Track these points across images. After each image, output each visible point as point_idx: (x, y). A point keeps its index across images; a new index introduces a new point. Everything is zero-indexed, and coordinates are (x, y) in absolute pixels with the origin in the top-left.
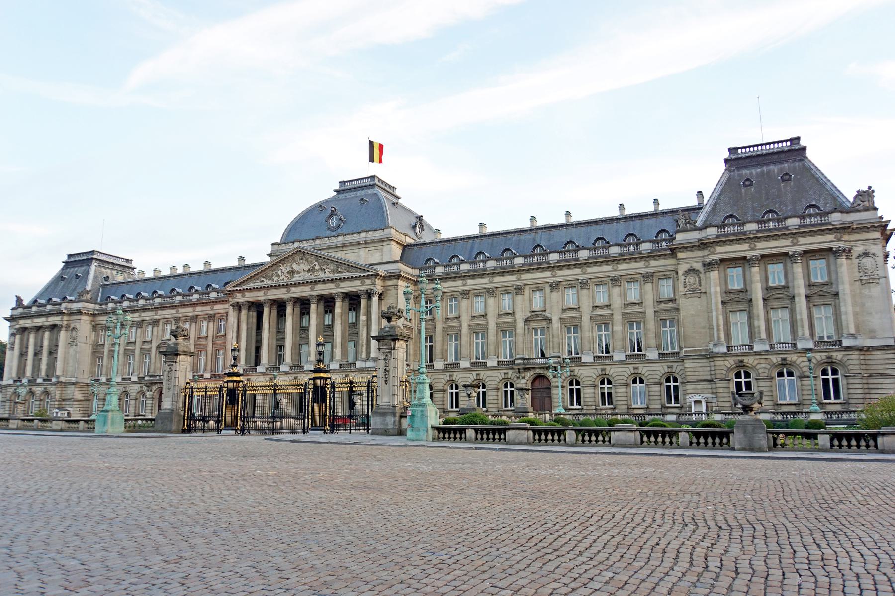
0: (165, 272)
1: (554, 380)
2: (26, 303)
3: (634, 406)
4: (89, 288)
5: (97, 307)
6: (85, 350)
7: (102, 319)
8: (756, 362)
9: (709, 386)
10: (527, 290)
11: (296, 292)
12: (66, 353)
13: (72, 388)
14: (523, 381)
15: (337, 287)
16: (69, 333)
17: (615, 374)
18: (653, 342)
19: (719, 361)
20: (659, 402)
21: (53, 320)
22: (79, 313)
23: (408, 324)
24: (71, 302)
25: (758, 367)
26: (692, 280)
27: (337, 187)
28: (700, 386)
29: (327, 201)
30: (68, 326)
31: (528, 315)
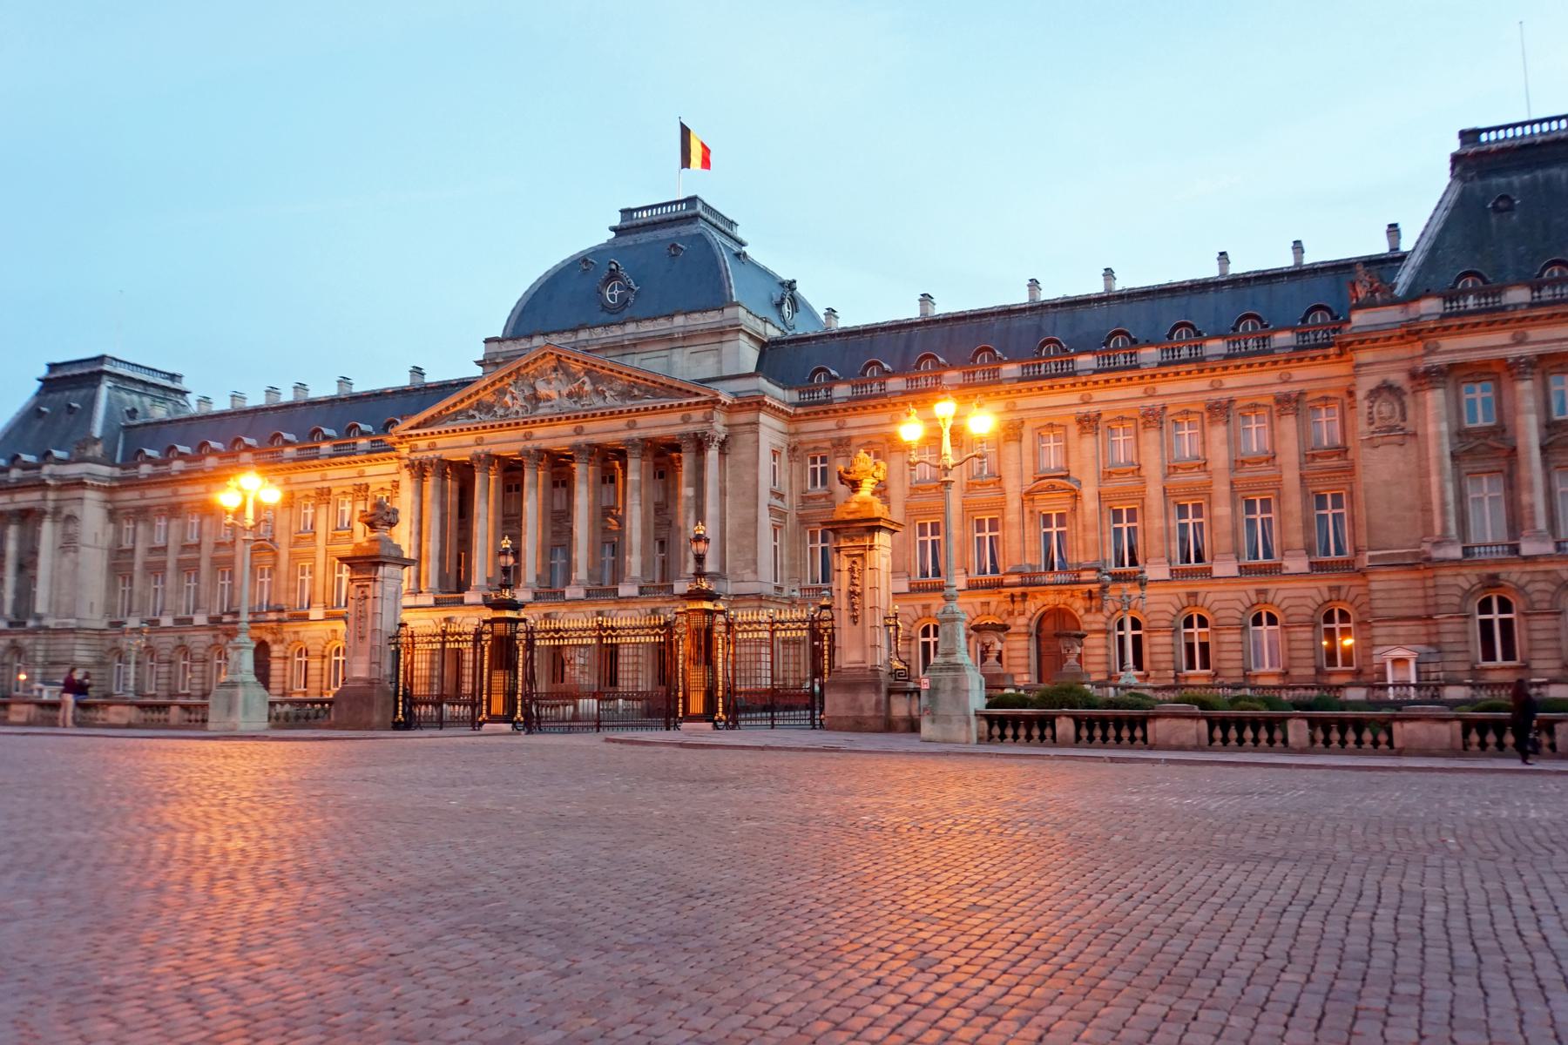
0: (256, 399)
1: (1088, 618)
3: (1255, 671)
4: (97, 431)
5: (117, 472)
6: (93, 562)
7: (130, 497)
8: (1526, 578)
9: (1423, 630)
13: (70, 638)
14: (1022, 621)
15: (631, 426)
16: (59, 526)
17: (1216, 605)
18: (1297, 539)
19: (1446, 577)
20: (1311, 662)
21: (24, 500)
22: (80, 484)
23: (778, 503)
24: (60, 462)
25: (1530, 588)
26: (1386, 409)
28: (1402, 629)
29: (597, 252)
30: (57, 512)
31: (1029, 483)
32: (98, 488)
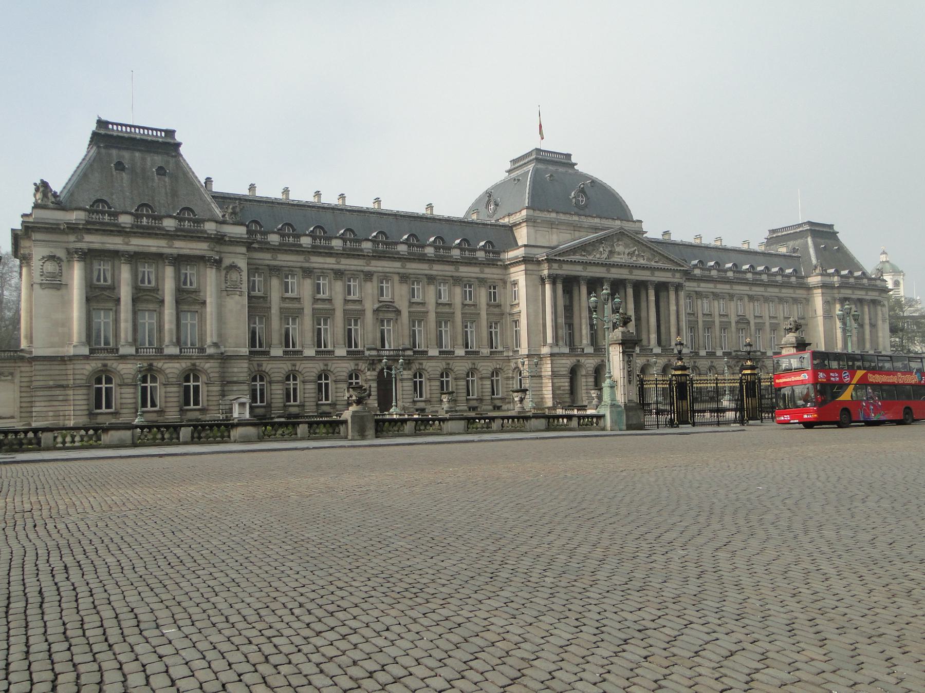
7: (265, 258)
11: (615, 274)
12: (220, 307)
15: (653, 275)
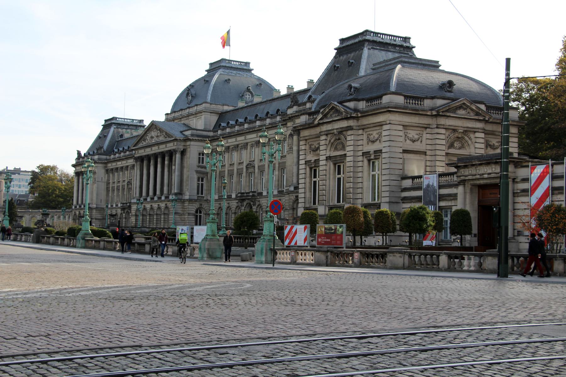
2: (83, 155)
10: (249, 147)
23: (203, 170)
27: (208, 67)
32: (101, 163)
